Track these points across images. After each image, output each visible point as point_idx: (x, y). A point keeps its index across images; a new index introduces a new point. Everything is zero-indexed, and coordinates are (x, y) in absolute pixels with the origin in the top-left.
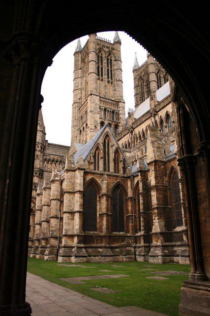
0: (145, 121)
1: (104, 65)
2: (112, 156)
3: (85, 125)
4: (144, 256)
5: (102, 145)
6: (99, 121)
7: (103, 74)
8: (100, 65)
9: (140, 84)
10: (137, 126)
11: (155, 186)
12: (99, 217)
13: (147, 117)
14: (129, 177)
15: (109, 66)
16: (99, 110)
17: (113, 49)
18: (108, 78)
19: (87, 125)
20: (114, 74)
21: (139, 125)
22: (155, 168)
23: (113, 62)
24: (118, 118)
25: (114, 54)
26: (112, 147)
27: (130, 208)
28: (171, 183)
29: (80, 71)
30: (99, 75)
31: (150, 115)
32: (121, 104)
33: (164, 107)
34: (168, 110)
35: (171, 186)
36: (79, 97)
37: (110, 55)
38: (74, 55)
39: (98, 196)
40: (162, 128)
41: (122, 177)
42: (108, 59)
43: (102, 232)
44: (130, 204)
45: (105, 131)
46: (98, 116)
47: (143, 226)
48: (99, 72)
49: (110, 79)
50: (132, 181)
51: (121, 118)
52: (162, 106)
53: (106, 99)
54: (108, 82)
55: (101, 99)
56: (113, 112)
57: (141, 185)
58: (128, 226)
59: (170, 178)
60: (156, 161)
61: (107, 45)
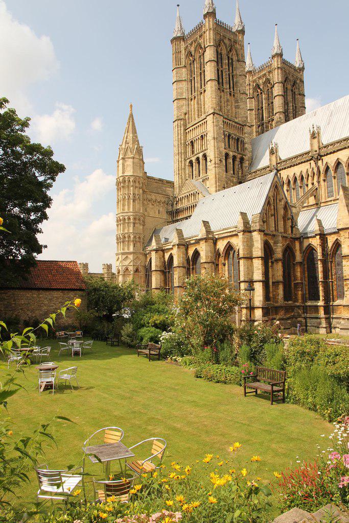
0: (299, 164)
1: (224, 67)
2: (282, 212)
3: (200, 155)
4: (326, 328)
5: (272, 198)
6: (224, 152)
7: (224, 82)
8: (220, 67)
9: (256, 94)
10: (285, 168)
12: (273, 285)
13: (303, 160)
14: (297, 239)
15: (231, 69)
16: (223, 137)
17: (235, 42)
18: (230, 89)
19: (205, 156)
20: (237, 82)
21: (288, 167)
23: (234, 63)
24: (244, 149)
25: (236, 51)
26: (280, 201)
27: (299, 274)
29: (184, 70)
30: (219, 83)
32: (247, 129)
33: (334, 152)
34: (340, 157)
36: (185, 111)
37: (230, 51)
38: (172, 41)
39: (270, 261)
41: (291, 238)
42: (228, 57)
43: (277, 302)
44: (299, 270)
45: (274, 181)
46: (223, 145)
47: (322, 296)
48: (219, 80)
49: (232, 90)
50: (301, 244)
51: (246, 149)
52: (331, 149)
53: (230, 120)
54: (230, 94)
55: (225, 120)
56: (238, 139)
57: (319, 250)
58: (296, 295)
61: (228, 35)
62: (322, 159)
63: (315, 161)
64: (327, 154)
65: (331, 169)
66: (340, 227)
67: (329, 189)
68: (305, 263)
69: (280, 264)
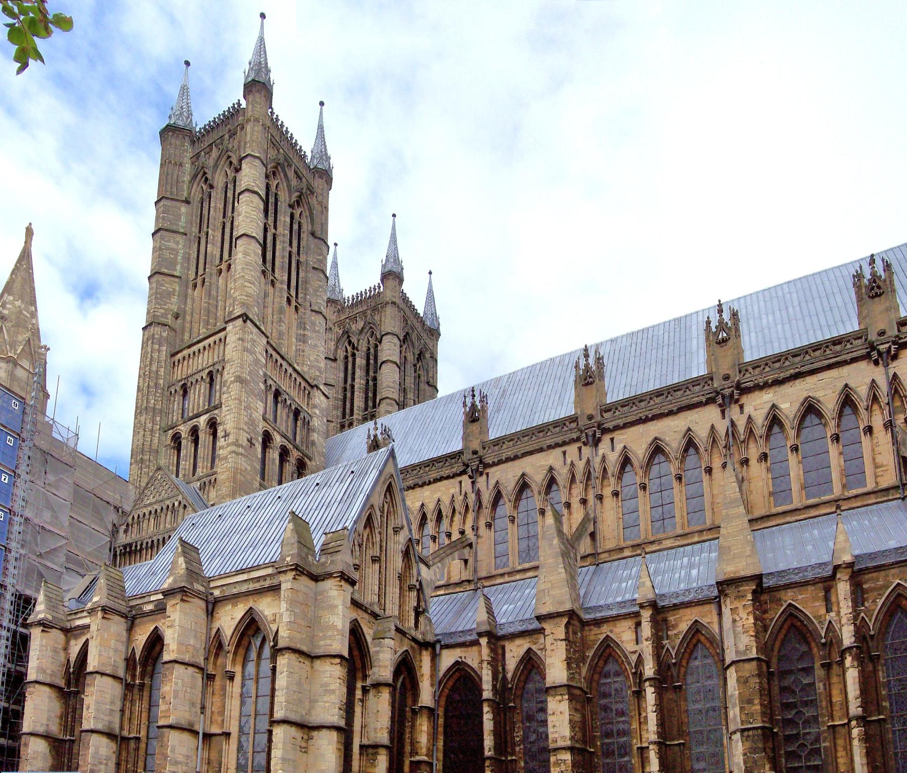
11: (568, 686)
22: (567, 633)
28: (594, 684)
31: (458, 468)
35: (594, 692)
40: (493, 518)
59: (593, 669)
60: (571, 615)
62: (487, 474)
63: (470, 477)
64: (500, 462)
65: (506, 497)
66: (544, 611)
67: (499, 547)
68: (441, 712)
69: (385, 695)
